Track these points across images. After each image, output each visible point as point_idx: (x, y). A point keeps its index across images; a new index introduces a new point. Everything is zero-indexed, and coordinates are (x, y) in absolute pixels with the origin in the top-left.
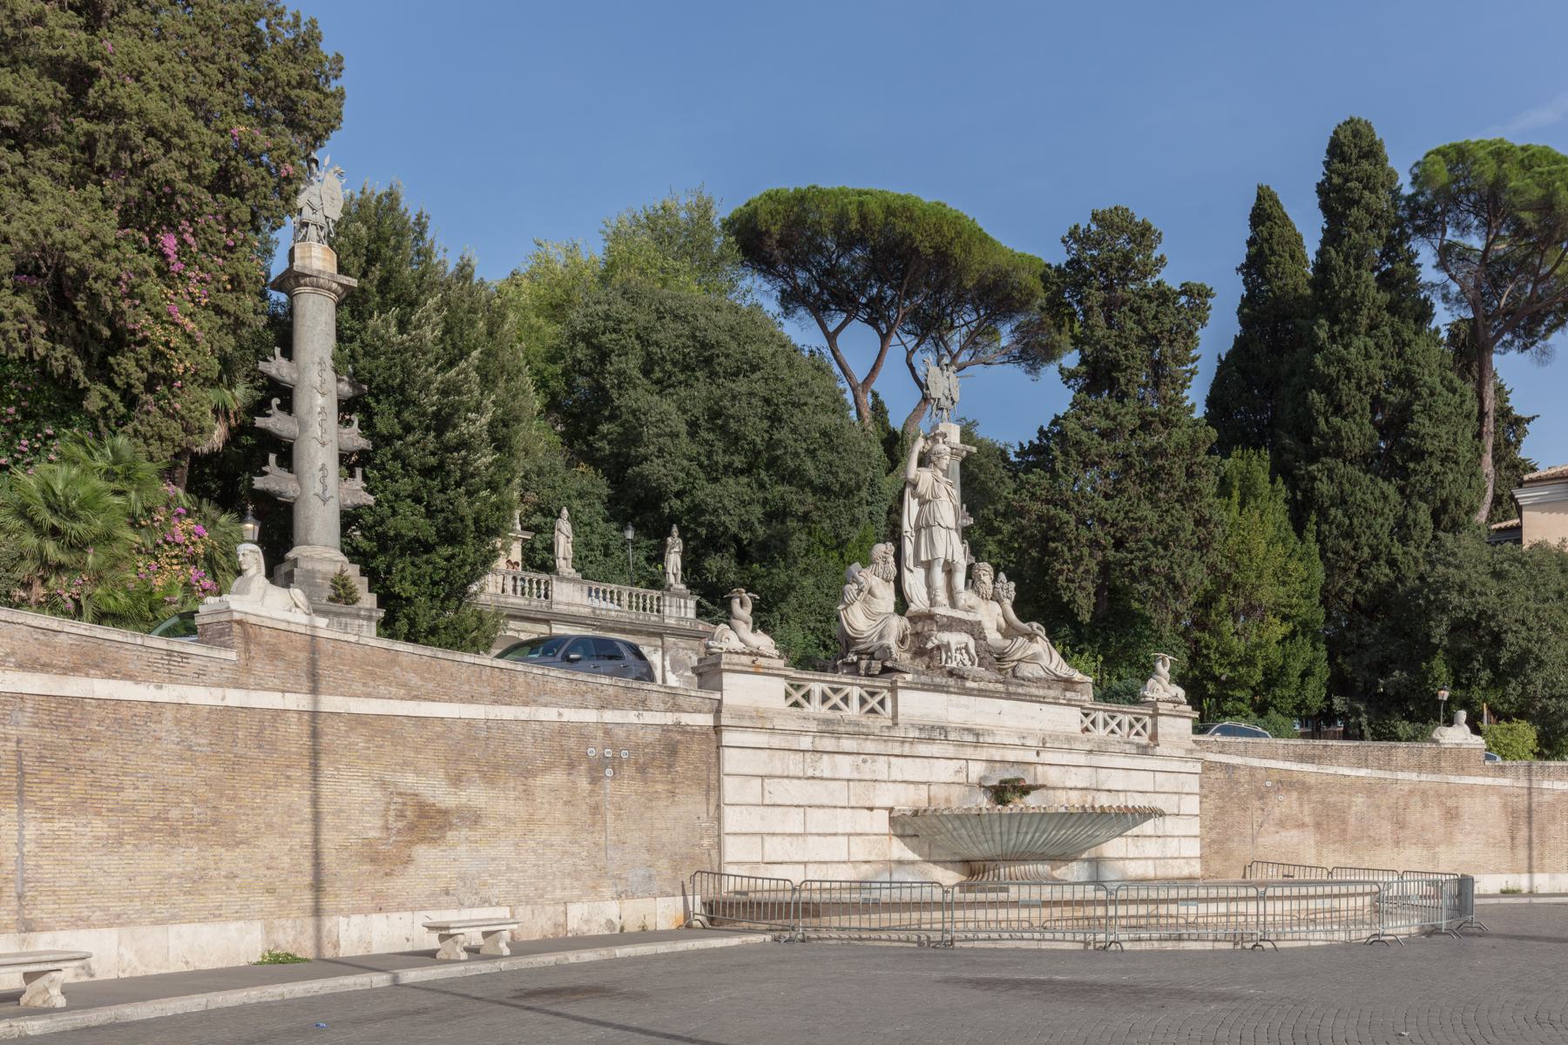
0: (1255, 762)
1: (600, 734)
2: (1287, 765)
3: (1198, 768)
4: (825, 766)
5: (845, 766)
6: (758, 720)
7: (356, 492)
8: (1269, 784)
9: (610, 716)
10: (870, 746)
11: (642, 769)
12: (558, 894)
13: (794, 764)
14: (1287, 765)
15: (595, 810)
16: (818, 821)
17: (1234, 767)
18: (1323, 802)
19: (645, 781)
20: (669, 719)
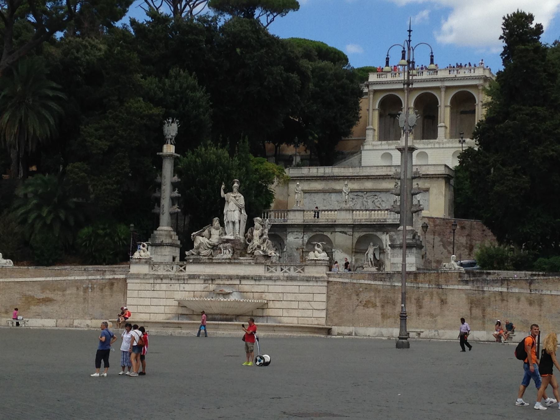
0: (355, 281)
1: (88, 282)
2: (369, 282)
3: (326, 284)
4: (157, 287)
5: (164, 287)
6: (137, 276)
7: (176, 209)
8: (361, 289)
9: (90, 277)
10: (173, 281)
11: (102, 290)
12: (71, 317)
13: (148, 287)
14: (369, 282)
15: (85, 299)
16: (155, 301)
17: (346, 283)
18: (386, 296)
19: (102, 292)
20: (111, 277)
